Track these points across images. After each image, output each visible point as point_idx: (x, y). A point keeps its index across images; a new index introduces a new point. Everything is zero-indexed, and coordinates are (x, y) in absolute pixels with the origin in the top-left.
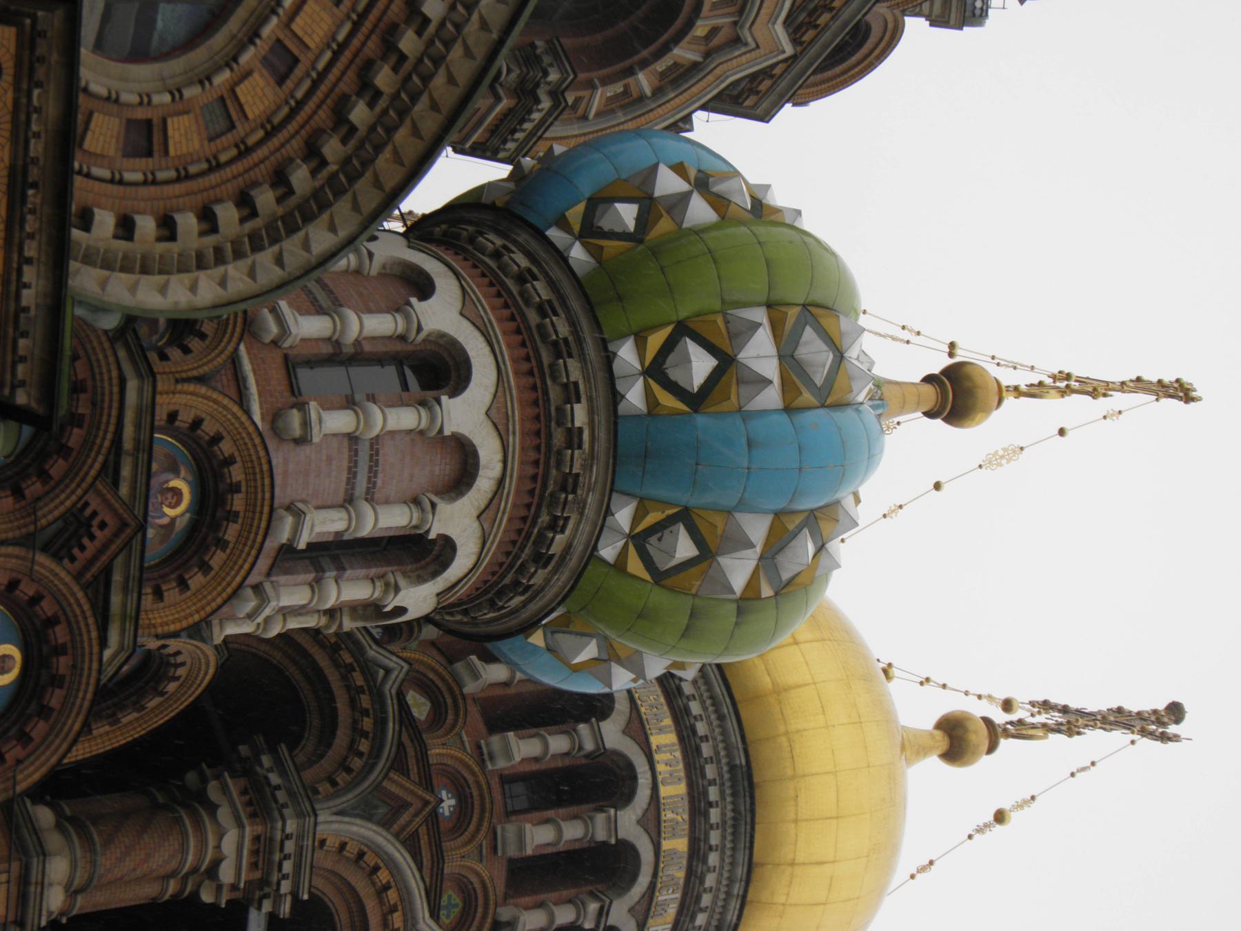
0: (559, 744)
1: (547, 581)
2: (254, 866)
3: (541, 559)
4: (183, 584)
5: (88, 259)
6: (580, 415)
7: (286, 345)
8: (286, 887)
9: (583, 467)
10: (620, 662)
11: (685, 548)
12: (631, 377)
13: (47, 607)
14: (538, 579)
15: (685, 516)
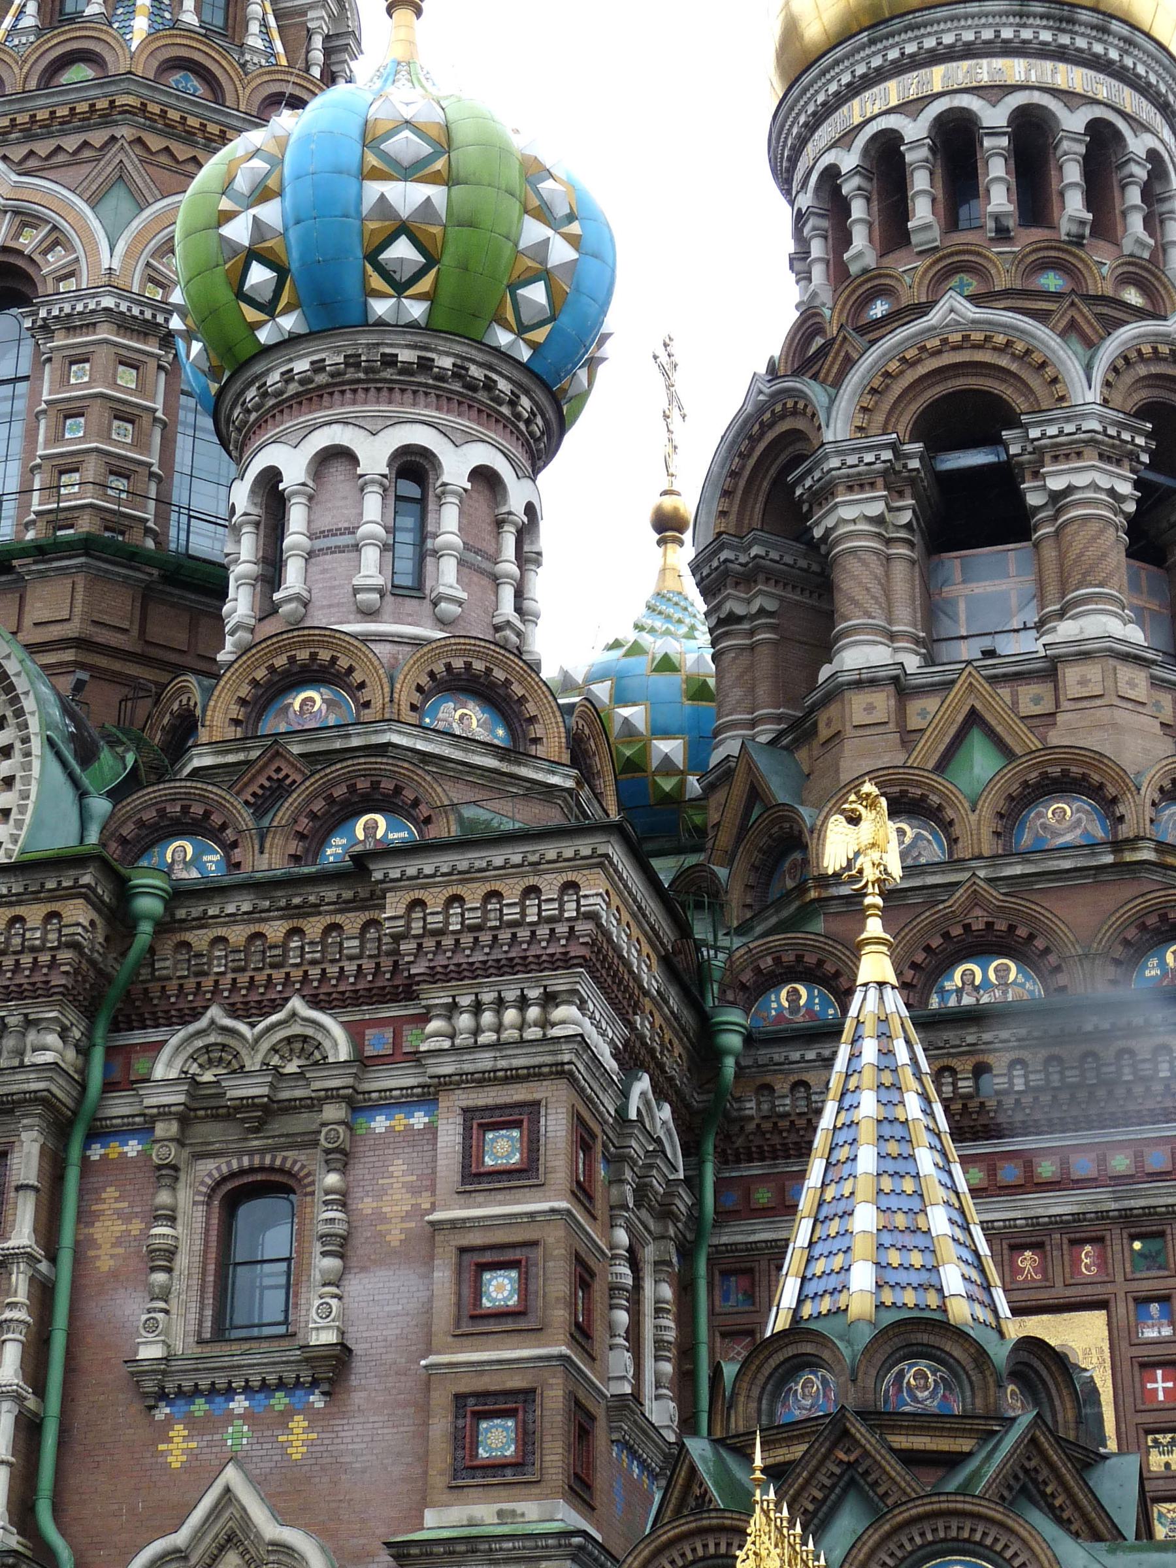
0: (858, 209)
1: (448, 354)
2: (872, 485)
3: (425, 365)
4: (362, 685)
5: (15, 842)
6: (301, 366)
7: (253, 622)
8: (887, 455)
9: (339, 353)
10: (544, 261)
11: (402, 250)
12: (279, 327)
13: (318, 806)
14: (447, 362)
15: (372, 257)
